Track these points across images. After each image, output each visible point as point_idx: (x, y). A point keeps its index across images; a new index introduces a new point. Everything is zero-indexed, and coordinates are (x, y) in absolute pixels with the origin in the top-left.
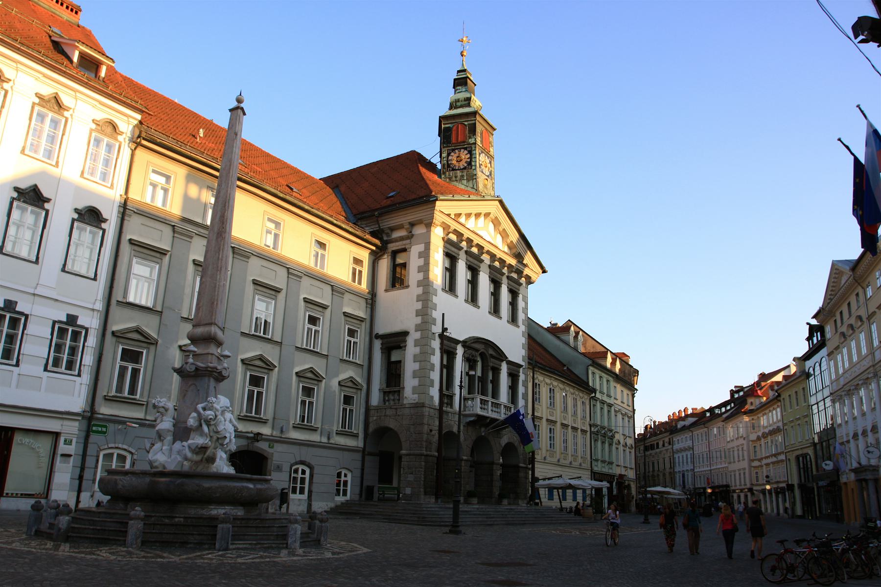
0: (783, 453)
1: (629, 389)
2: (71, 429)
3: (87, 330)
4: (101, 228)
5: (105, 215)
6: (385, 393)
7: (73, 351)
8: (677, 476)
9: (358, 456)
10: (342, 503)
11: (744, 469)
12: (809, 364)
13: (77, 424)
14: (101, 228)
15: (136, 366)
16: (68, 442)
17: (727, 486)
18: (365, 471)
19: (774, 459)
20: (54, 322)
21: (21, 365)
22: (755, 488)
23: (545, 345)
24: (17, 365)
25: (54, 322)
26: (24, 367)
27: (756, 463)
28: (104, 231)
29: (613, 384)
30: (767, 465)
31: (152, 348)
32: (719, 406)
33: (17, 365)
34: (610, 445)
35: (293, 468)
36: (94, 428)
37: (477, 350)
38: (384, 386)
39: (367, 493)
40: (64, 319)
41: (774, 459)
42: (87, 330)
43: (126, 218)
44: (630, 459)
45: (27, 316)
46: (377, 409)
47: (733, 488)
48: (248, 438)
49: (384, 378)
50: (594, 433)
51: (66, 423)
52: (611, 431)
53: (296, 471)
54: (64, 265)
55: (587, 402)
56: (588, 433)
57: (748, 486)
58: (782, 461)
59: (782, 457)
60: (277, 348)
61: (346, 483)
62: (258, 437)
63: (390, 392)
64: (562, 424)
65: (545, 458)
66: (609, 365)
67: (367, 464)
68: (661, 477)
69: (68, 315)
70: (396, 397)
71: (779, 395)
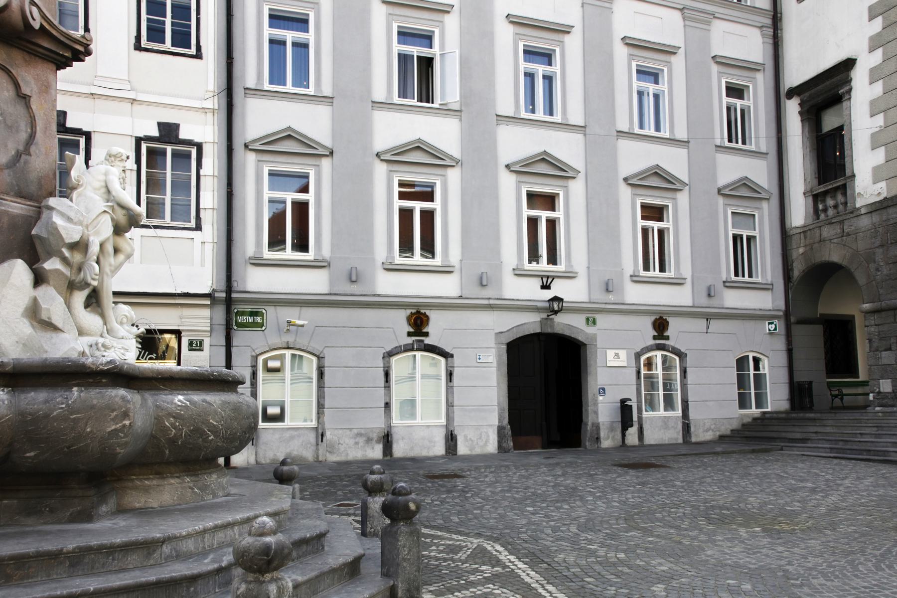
2: (198, 321)
3: (199, 147)
6: (817, 198)
7: (181, 186)
9: (779, 325)
10: (755, 419)
13: (206, 312)
15: (302, 197)
16: (196, 346)
18: (796, 355)
20: (139, 141)
25: (139, 141)
31: (326, 163)
35: (643, 358)
36: (240, 319)
38: (816, 182)
39: (800, 393)
40: (155, 133)
42: (199, 147)
45: (88, 136)
46: (805, 231)
48: (537, 309)
49: (812, 168)
53: (649, 364)
54: (138, 38)
60: (579, 137)
61: (759, 379)
63: (825, 193)
67: (795, 340)
69: (160, 125)
70: (840, 198)
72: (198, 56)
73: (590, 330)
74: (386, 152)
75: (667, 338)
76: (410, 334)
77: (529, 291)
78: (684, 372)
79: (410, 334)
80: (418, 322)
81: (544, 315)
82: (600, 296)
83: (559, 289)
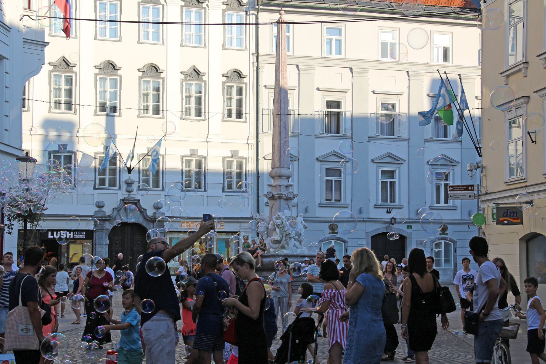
3: (246, 159)
4: (244, 83)
5: (245, 72)
14: (244, 83)
20: (224, 158)
21: (208, 190)
24: (205, 191)
25: (224, 158)
26: (210, 192)
28: (246, 84)
31: (296, 163)
33: (205, 191)
42: (246, 159)
43: (260, 70)
48: (385, 222)
51: (242, 224)
60: (406, 144)
62: (393, 221)
69: (231, 151)
72: (245, 121)
73: (409, 231)
74: (321, 157)
75: (447, 234)
76: (329, 233)
77: (382, 214)
78: (455, 250)
79: (329, 233)
80: (333, 229)
81: (388, 225)
82: (413, 216)
83: (394, 214)
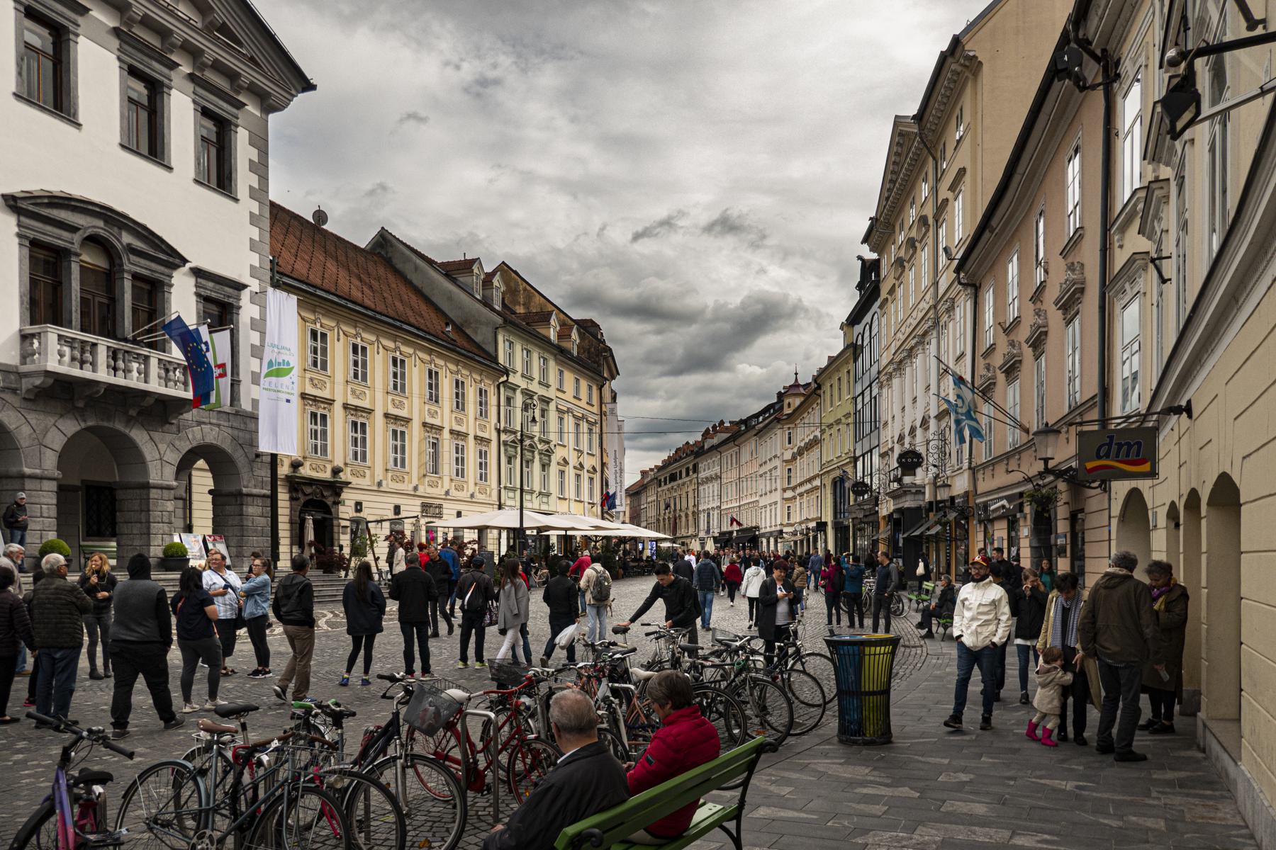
0: (818, 475)
1: (592, 379)
8: (701, 516)
11: (776, 503)
12: (858, 328)
17: (757, 528)
19: (808, 486)
22: (785, 530)
23: (427, 291)
27: (789, 494)
29: (553, 367)
30: (801, 495)
32: (756, 416)
34: (544, 467)
37: (73, 229)
41: (808, 486)
44: (591, 490)
47: (763, 531)
50: (505, 443)
52: (548, 442)
55: (492, 392)
56: (494, 444)
57: (778, 528)
58: (816, 488)
59: (817, 482)
64: (425, 424)
65: (380, 484)
66: (553, 335)
68: (683, 519)
71: (819, 387)
